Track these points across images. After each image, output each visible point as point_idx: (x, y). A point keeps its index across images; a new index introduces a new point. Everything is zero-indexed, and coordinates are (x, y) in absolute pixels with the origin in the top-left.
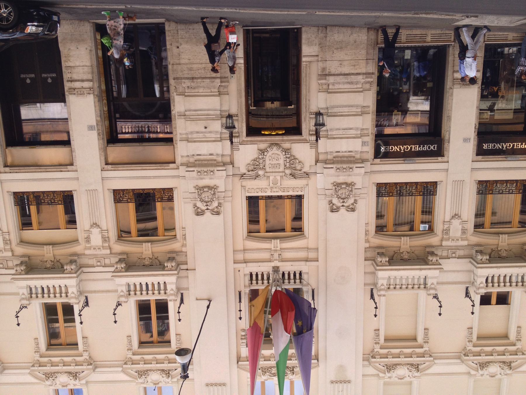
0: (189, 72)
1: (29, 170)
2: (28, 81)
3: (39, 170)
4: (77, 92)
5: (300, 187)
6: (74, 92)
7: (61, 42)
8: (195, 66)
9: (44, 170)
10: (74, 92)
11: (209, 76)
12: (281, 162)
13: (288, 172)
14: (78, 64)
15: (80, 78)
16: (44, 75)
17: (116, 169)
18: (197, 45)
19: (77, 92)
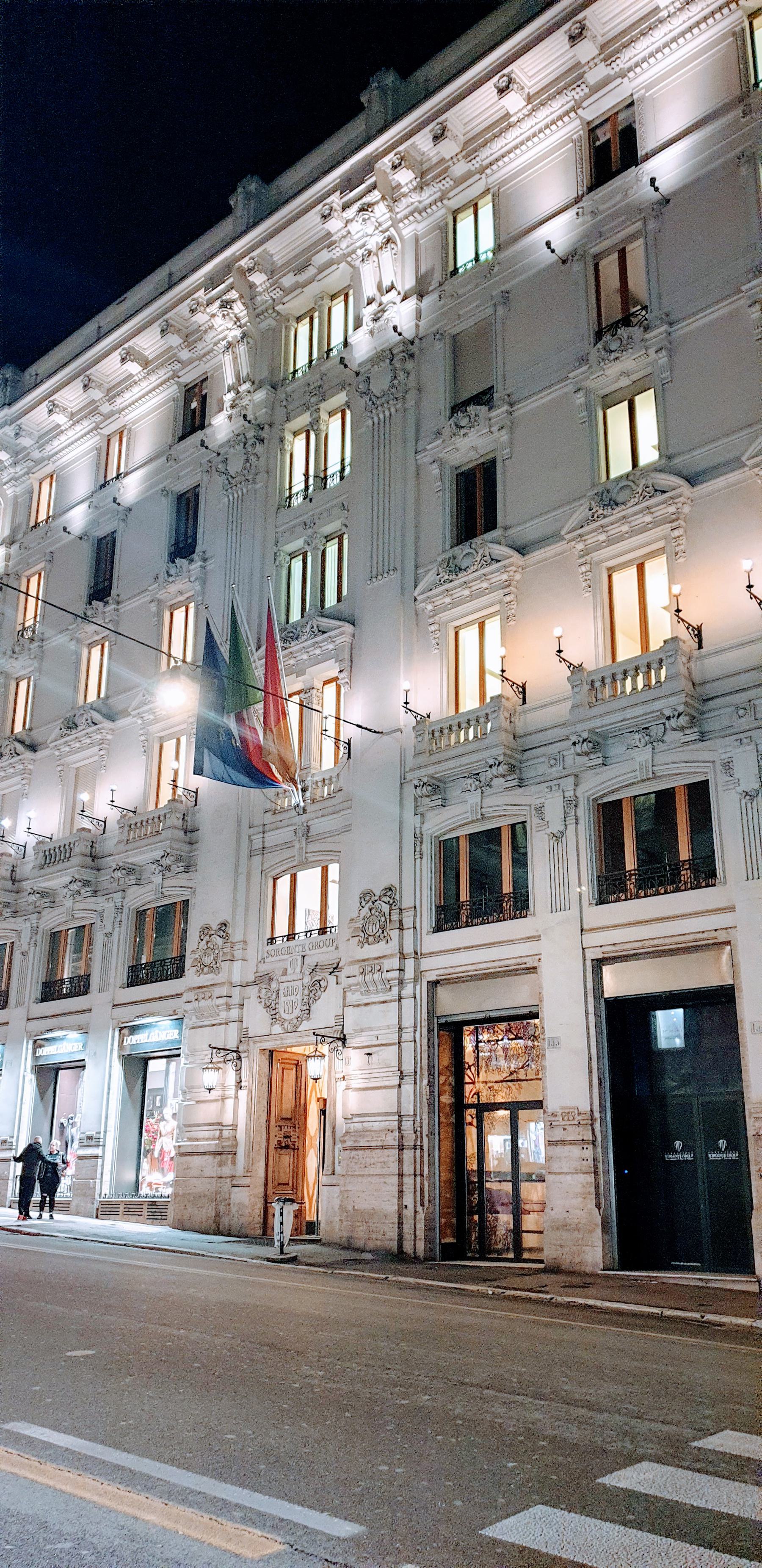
0: (386, 1159)
1: (678, 939)
2: (722, 1144)
3: (656, 942)
4: (574, 1119)
5: (270, 959)
6: (580, 1118)
7: (596, 1225)
8: (378, 1171)
9: (647, 943)
10: (580, 1118)
11: (361, 1153)
12: (282, 999)
13: (274, 985)
14: (569, 1177)
15: (568, 1148)
16: (689, 1157)
17: (519, 960)
18: (373, 1209)
19: (574, 1119)
